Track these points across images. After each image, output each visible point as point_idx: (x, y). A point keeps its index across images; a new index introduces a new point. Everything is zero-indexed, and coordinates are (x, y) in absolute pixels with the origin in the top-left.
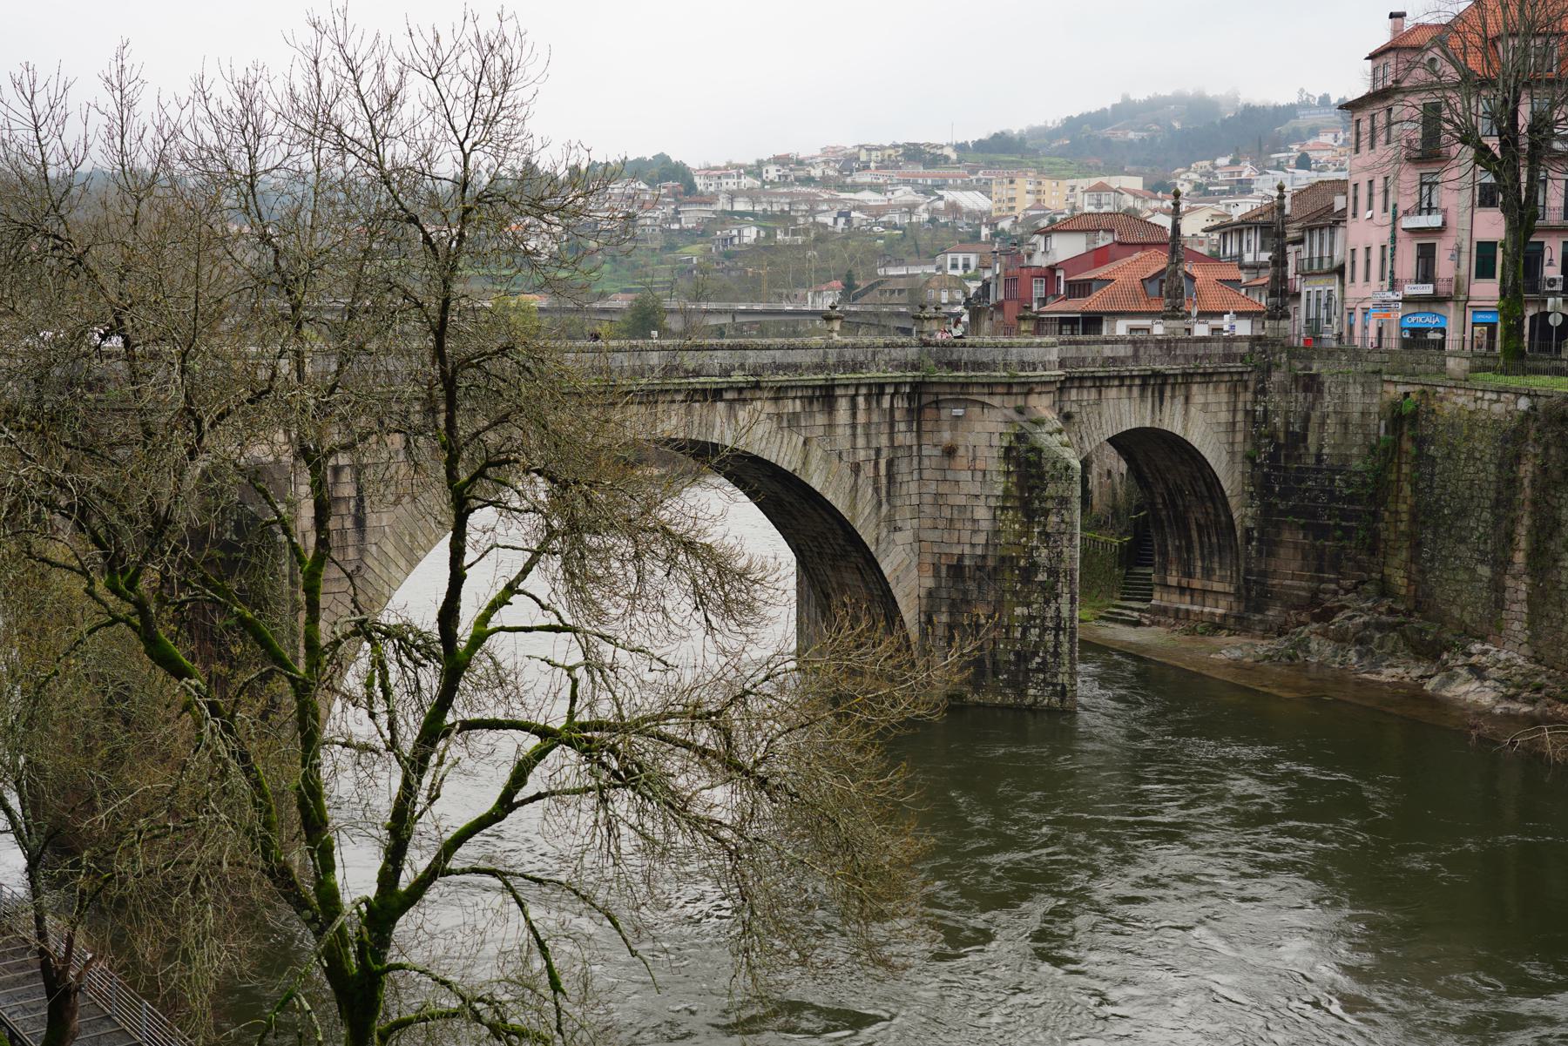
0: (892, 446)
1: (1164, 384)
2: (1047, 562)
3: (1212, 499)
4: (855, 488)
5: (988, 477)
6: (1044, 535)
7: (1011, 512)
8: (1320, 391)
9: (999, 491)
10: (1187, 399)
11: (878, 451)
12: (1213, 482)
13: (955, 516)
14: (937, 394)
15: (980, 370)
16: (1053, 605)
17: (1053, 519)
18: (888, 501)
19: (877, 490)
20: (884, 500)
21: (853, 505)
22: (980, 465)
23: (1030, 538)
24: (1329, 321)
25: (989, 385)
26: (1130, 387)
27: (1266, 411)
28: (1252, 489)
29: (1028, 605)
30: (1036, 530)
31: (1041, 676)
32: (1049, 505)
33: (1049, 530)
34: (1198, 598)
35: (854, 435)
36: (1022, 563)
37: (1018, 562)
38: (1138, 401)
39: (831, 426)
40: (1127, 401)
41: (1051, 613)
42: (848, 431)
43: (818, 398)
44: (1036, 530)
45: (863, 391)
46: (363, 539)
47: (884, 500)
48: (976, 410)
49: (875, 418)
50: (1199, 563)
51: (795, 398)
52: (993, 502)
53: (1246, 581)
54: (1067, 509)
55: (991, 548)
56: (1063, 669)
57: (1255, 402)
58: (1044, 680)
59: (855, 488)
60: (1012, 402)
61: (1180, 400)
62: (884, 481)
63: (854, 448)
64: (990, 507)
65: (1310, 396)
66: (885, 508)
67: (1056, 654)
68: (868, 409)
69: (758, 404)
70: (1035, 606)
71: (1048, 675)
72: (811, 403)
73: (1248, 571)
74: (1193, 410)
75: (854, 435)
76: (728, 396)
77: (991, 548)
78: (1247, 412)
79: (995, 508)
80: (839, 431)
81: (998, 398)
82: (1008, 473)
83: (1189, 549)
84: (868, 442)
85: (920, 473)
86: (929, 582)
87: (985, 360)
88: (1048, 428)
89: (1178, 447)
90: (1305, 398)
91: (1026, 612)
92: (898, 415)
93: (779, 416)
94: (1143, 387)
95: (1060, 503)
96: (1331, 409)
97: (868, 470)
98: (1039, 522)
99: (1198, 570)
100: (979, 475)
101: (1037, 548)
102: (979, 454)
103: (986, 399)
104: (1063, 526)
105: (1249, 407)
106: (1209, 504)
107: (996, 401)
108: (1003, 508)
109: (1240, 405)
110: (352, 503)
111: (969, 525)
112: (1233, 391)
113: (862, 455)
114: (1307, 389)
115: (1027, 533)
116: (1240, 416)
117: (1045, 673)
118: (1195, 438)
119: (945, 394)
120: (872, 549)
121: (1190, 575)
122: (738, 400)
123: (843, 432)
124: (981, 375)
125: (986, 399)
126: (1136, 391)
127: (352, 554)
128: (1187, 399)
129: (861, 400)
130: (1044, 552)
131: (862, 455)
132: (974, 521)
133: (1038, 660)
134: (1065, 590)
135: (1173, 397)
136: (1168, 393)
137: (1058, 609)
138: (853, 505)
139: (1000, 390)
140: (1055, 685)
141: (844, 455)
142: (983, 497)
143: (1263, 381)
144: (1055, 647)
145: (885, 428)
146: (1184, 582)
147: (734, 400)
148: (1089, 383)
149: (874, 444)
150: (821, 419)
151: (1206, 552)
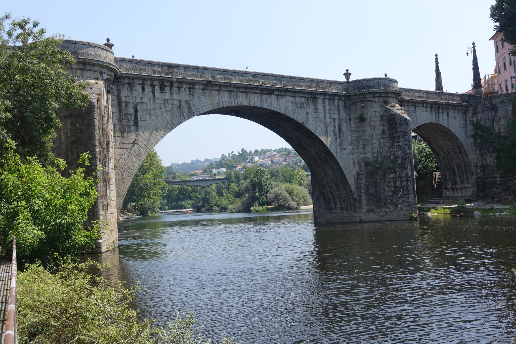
0: (339, 119)
1: (439, 108)
2: (401, 156)
3: (461, 153)
5: (376, 127)
6: (399, 146)
7: (386, 140)
8: (497, 110)
9: (380, 132)
10: (448, 114)
11: (334, 120)
12: (460, 147)
13: (365, 143)
14: (355, 100)
16: (405, 172)
17: (402, 140)
18: (339, 138)
19: (335, 134)
22: (373, 124)
23: (394, 148)
25: (373, 93)
26: (426, 107)
27: (477, 120)
28: (475, 148)
29: (395, 172)
30: (396, 145)
31: (403, 199)
32: (400, 134)
33: (400, 144)
34: (460, 192)
35: (325, 113)
36: (392, 157)
37: (390, 157)
38: (430, 113)
39: (316, 109)
40: (425, 113)
41: (404, 175)
42: (322, 112)
44: (396, 145)
47: (338, 138)
48: (370, 104)
49: (332, 108)
50: (458, 179)
52: (378, 136)
53: (477, 182)
54: (407, 135)
55: (379, 154)
56: (411, 196)
57: (473, 117)
58: (404, 201)
60: (382, 100)
61: (445, 114)
62: (337, 131)
63: (325, 117)
64: (378, 138)
65: (493, 112)
66: (338, 140)
67: (408, 190)
68: (329, 104)
69: (288, 98)
70: (398, 173)
71: (405, 199)
73: (478, 178)
74: (450, 119)
75: (325, 113)
76: (276, 93)
77: (379, 154)
78: (470, 121)
79: (380, 138)
80: (320, 111)
82: (383, 125)
83: (454, 174)
84: (330, 116)
85: (351, 130)
86: (358, 169)
87: (371, 85)
88: (396, 108)
89: (446, 133)
90: (491, 113)
91: (395, 176)
92: (341, 108)
93: (296, 103)
94: (431, 108)
95: (404, 134)
96: (502, 115)
98: (397, 142)
99: (459, 181)
100: (373, 127)
101: (397, 151)
103: (373, 99)
104: (406, 142)
106: (460, 155)
107: (377, 99)
108: (383, 138)
109: (468, 119)
110: (133, 116)
111: (370, 146)
112: (465, 113)
114: (492, 110)
115: (393, 146)
116: (468, 122)
117: (404, 198)
118: (452, 129)
119: (358, 99)
120: (335, 155)
121: (456, 184)
122: (280, 95)
123: (321, 111)
124: (370, 90)
125: (373, 99)
126: (429, 109)
128: (448, 114)
129: (326, 101)
130: (399, 152)
131: (328, 120)
132: (372, 144)
133: (401, 193)
134: (409, 166)
135: (443, 113)
136: (441, 111)
137: (407, 173)
139: (378, 95)
140: (408, 202)
142: (374, 136)
143: (475, 110)
144: (407, 188)
145: (336, 112)
146: (454, 187)
147: (278, 95)
148: (411, 104)
149: (333, 117)
150: (312, 106)
151: (461, 174)
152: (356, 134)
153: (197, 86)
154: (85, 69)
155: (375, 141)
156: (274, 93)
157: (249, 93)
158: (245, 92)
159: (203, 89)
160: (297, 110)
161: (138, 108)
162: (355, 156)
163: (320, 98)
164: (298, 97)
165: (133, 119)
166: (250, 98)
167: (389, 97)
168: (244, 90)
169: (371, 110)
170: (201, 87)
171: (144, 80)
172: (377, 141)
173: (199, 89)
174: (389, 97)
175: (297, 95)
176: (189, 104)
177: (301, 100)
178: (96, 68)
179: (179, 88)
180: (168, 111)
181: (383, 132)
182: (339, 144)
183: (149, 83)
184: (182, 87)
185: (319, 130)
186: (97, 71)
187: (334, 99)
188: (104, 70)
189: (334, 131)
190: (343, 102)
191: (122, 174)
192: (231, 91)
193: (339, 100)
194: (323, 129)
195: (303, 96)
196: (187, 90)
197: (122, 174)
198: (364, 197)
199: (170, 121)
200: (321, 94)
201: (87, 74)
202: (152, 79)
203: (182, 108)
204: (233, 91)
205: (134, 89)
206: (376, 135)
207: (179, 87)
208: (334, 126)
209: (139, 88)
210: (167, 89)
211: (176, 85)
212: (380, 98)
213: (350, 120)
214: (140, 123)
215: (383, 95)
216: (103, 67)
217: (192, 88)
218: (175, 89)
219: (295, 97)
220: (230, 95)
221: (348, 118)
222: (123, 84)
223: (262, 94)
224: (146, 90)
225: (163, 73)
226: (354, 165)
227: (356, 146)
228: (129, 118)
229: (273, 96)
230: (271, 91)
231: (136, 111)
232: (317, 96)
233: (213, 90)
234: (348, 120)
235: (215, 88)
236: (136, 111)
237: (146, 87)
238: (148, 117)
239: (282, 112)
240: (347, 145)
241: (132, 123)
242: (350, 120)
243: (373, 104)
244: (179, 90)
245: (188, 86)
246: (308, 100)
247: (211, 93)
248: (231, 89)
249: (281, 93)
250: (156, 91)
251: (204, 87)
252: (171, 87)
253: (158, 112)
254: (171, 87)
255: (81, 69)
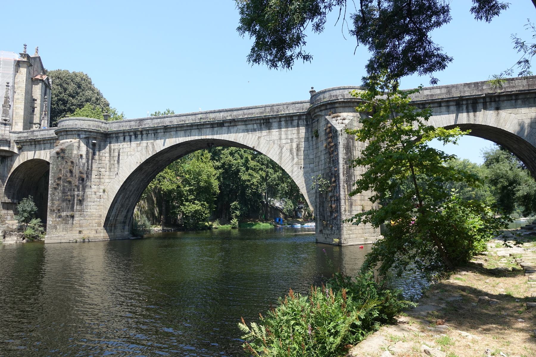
4: (281, 152)
11: (292, 140)
20: (295, 157)
21: (281, 158)
43: (264, 124)
45: (283, 119)
46: (119, 166)
47: (295, 157)
51: (253, 124)
59: (281, 152)
63: (280, 139)
69: (239, 127)
72: (261, 125)
76: (226, 125)
81: (324, 111)
103: (320, 113)
110: (117, 157)
113: (284, 141)
122: (231, 126)
125: (320, 113)
127: (116, 169)
131: (284, 141)
138: (281, 158)
139: (323, 108)
141: (276, 142)
147: (229, 126)
149: (290, 137)
153: (159, 131)
154: (67, 135)
155: (323, 158)
156: (223, 125)
157: (201, 128)
158: (198, 129)
159: (164, 132)
160: (248, 136)
161: (120, 152)
163: (274, 122)
164: (249, 124)
165: (117, 159)
166: (203, 132)
167: (337, 107)
168: (196, 127)
170: (162, 131)
171: (124, 133)
173: (160, 132)
174: (337, 107)
175: (247, 123)
176: (153, 145)
177: (253, 127)
178: (73, 133)
179: (147, 134)
180: (139, 151)
182: (296, 163)
183: (127, 134)
184: (149, 133)
185: (271, 152)
186: (75, 134)
187: (293, 120)
188: (80, 133)
189: (291, 150)
190: (305, 121)
191: (108, 195)
192: (185, 130)
193: (299, 119)
194: (277, 149)
195: (254, 122)
196: (153, 134)
197: (108, 195)
198: (318, 217)
199: (139, 159)
200: (275, 118)
201: (68, 136)
202: (129, 132)
203: (148, 148)
204: (187, 130)
205: (119, 140)
207: (147, 133)
208: (292, 146)
209: (122, 138)
210: (140, 136)
211: (144, 132)
212: (326, 111)
213: (312, 137)
214: (121, 161)
215: (328, 107)
216: (79, 131)
217: (156, 133)
218: (145, 135)
219: (246, 125)
220: (185, 132)
221: (310, 136)
222: (113, 137)
223: (213, 127)
224: (126, 139)
225: (136, 126)
228: (115, 159)
229: (224, 128)
230: (220, 125)
231: (119, 155)
232: (271, 121)
233: (171, 131)
234: (310, 138)
235: (172, 130)
236: (119, 155)
237: (126, 137)
238: (126, 157)
239: (232, 140)
240: (308, 163)
241: (116, 162)
242: (312, 137)
244: (147, 136)
245: (152, 132)
246: (261, 125)
247: (170, 134)
248: (185, 129)
249: (231, 124)
250: (132, 139)
251: (164, 130)
252: (142, 134)
253: (133, 153)
254: (142, 134)
255: (65, 135)
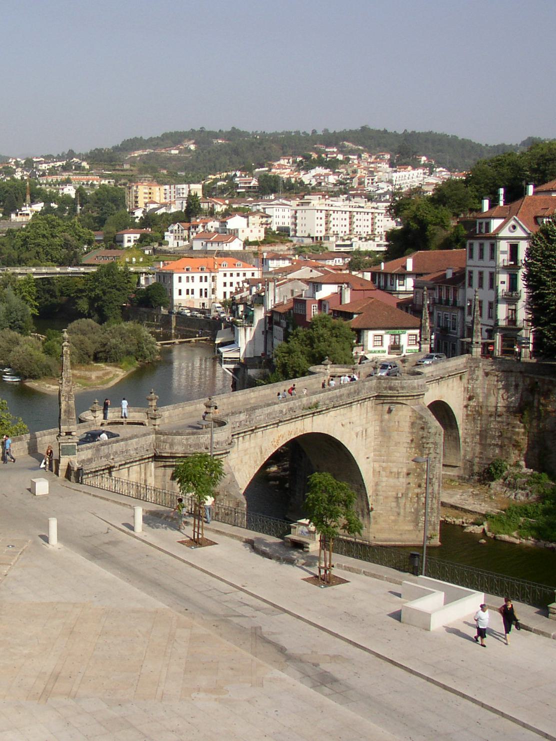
10: (448, 385)
15: (403, 390)
24: (454, 329)
27: (473, 387)
61: (445, 387)
64: (405, 447)
78: (465, 388)
79: (407, 448)
87: (405, 385)
97: (360, 434)
102: (400, 425)
103: (404, 402)
105: (466, 386)
107: (408, 402)
128: (448, 385)
137: (433, 489)
152: (380, 439)
162: (376, 465)
169: (400, 413)
172: (405, 450)
181: (412, 441)
206: (404, 443)
226: (374, 474)
227: (377, 453)
243: (404, 406)
